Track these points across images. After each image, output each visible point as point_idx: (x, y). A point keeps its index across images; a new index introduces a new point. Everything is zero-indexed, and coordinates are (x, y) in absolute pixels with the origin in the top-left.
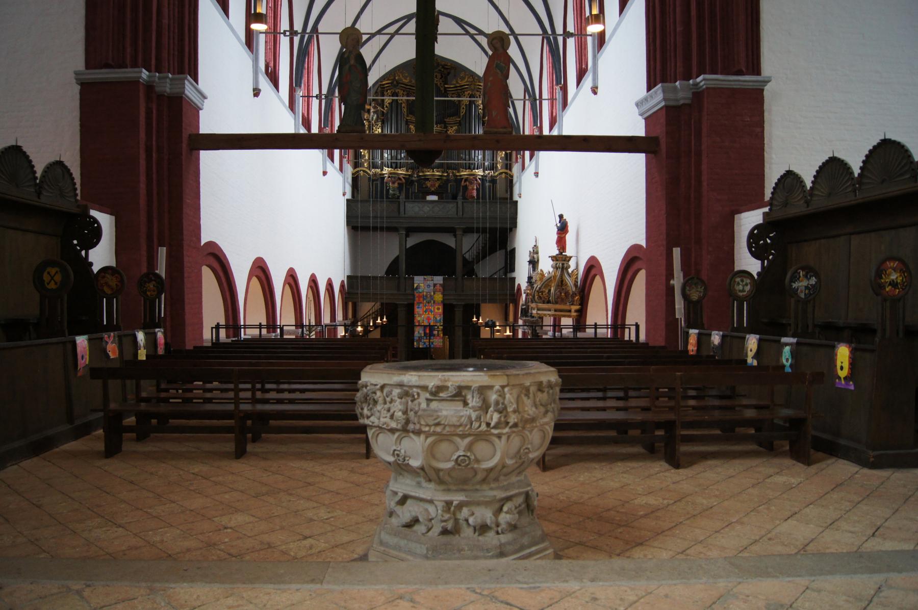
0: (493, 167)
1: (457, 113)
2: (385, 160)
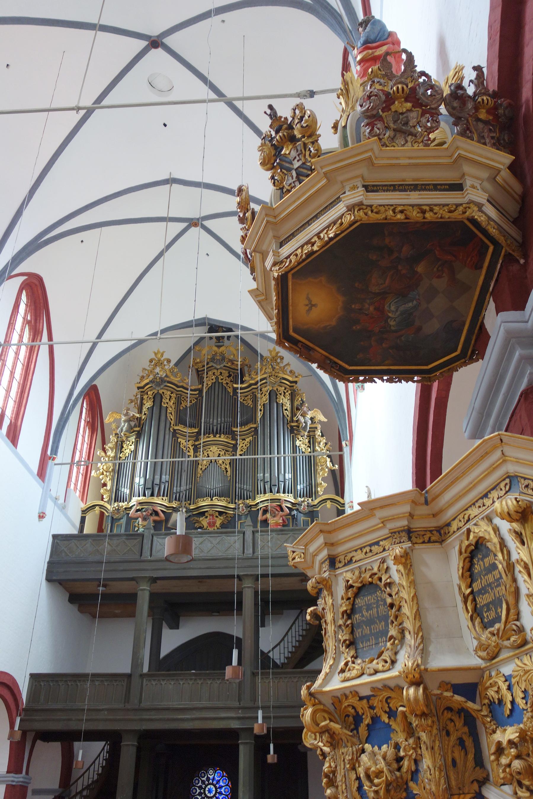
0: (311, 493)
1: (252, 419)
2: (136, 486)
